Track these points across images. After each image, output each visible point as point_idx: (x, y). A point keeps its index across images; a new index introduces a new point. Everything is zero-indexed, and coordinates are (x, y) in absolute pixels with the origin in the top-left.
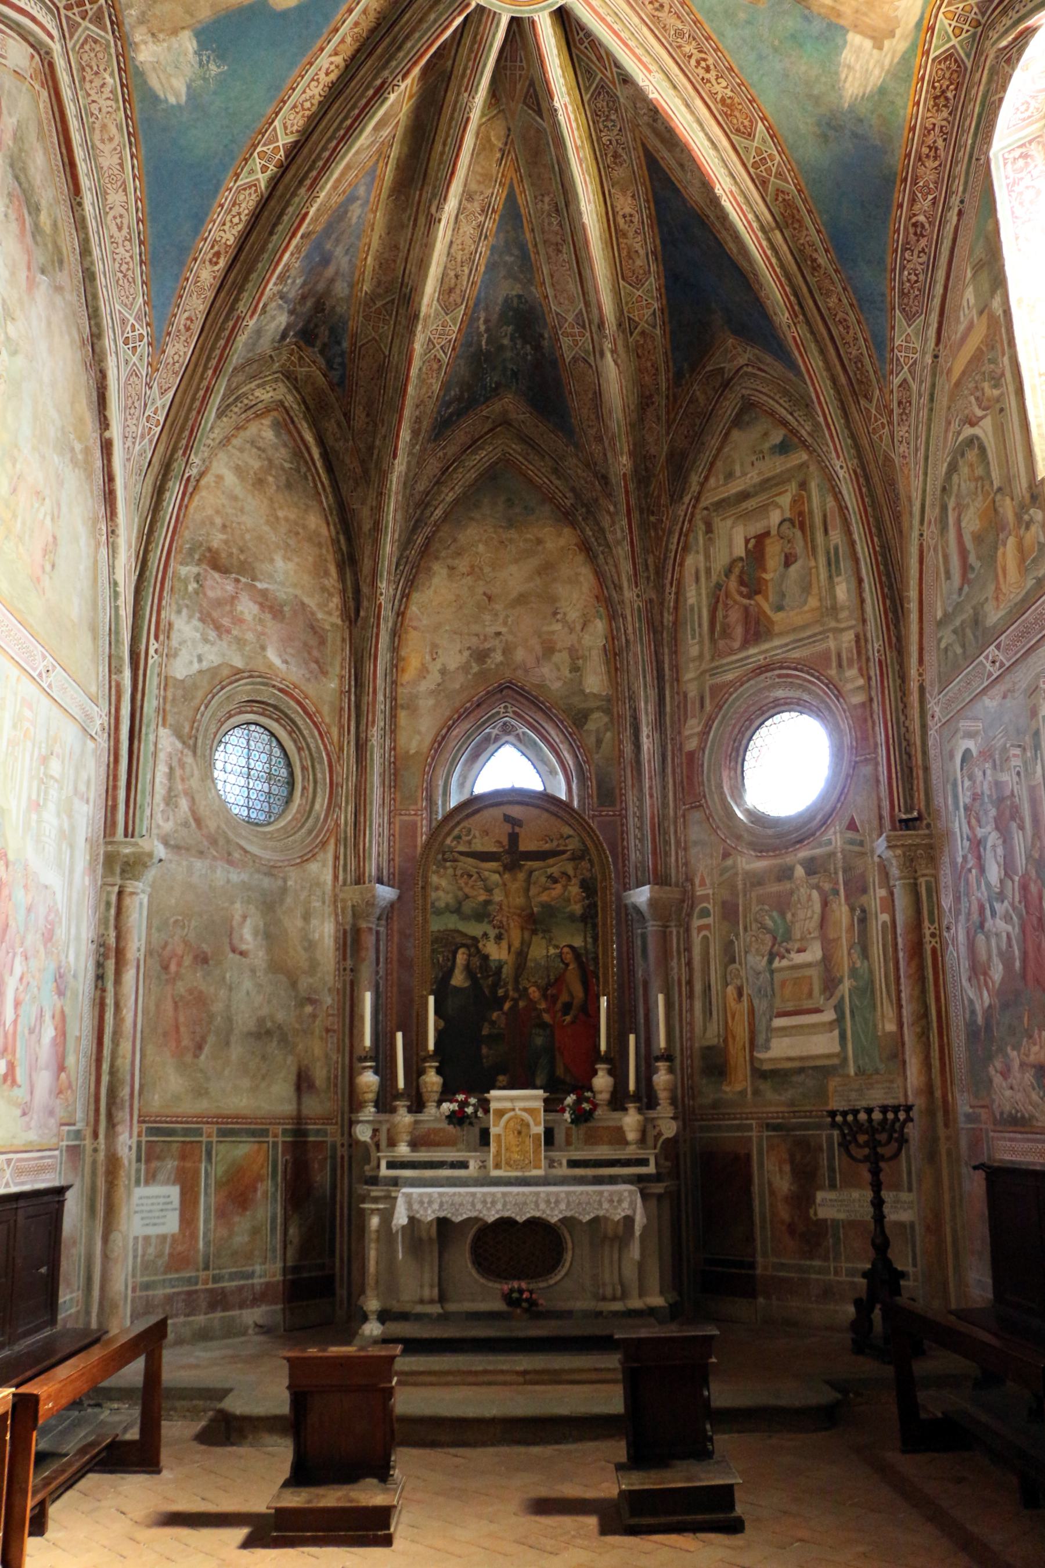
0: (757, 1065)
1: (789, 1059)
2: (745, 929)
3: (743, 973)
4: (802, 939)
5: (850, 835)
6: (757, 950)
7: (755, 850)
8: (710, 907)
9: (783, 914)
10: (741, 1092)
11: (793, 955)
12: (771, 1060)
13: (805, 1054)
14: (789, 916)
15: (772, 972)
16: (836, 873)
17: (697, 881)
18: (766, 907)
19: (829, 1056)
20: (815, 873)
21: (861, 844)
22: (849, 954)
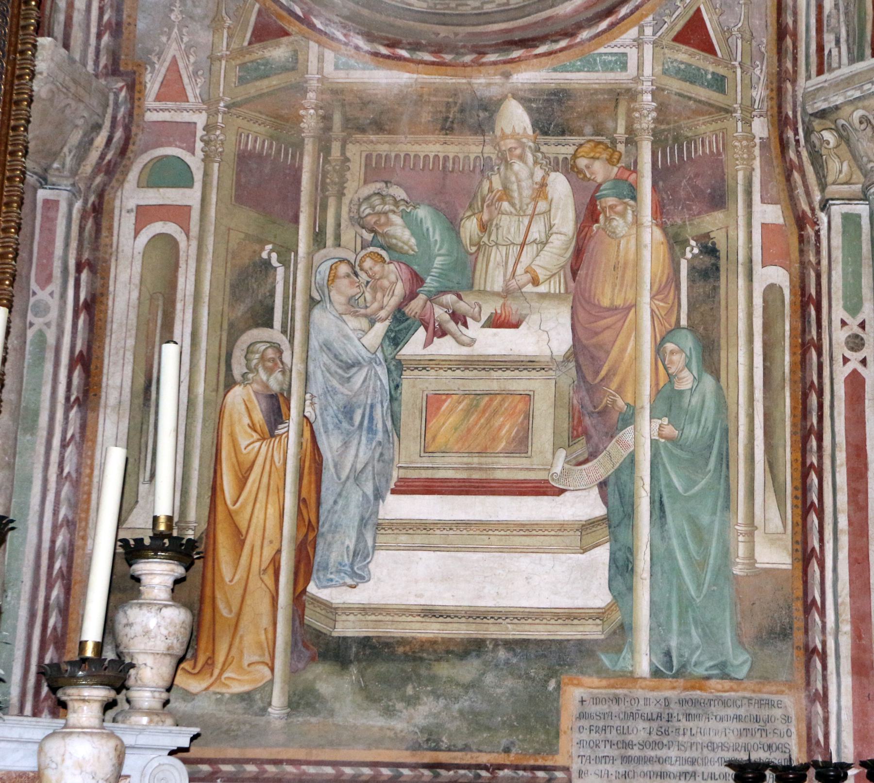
0: (312, 618)
1: (431, 613)
2: (318, 239)
3: (294, 359)
4: (507, 293)
5: (684, 55)
6: (351, 301)
7: (370, 37)
8: (195, 162)
9: (453, 225)
10: (246, 697)
11: (474, 330)
12: (365, 610)
13: (487, 602)
14: (470, 227)
15: (397, 367)
16: (631, 140)
17: (152, 83)
18: (400, 193)
19: (570, 616)
20: (564, 131)
21: (719, 83)
22: (659, 350)
